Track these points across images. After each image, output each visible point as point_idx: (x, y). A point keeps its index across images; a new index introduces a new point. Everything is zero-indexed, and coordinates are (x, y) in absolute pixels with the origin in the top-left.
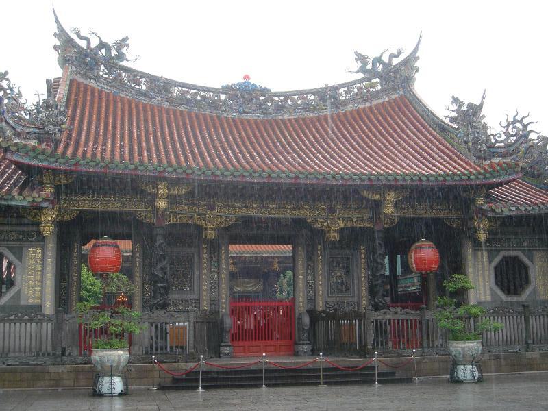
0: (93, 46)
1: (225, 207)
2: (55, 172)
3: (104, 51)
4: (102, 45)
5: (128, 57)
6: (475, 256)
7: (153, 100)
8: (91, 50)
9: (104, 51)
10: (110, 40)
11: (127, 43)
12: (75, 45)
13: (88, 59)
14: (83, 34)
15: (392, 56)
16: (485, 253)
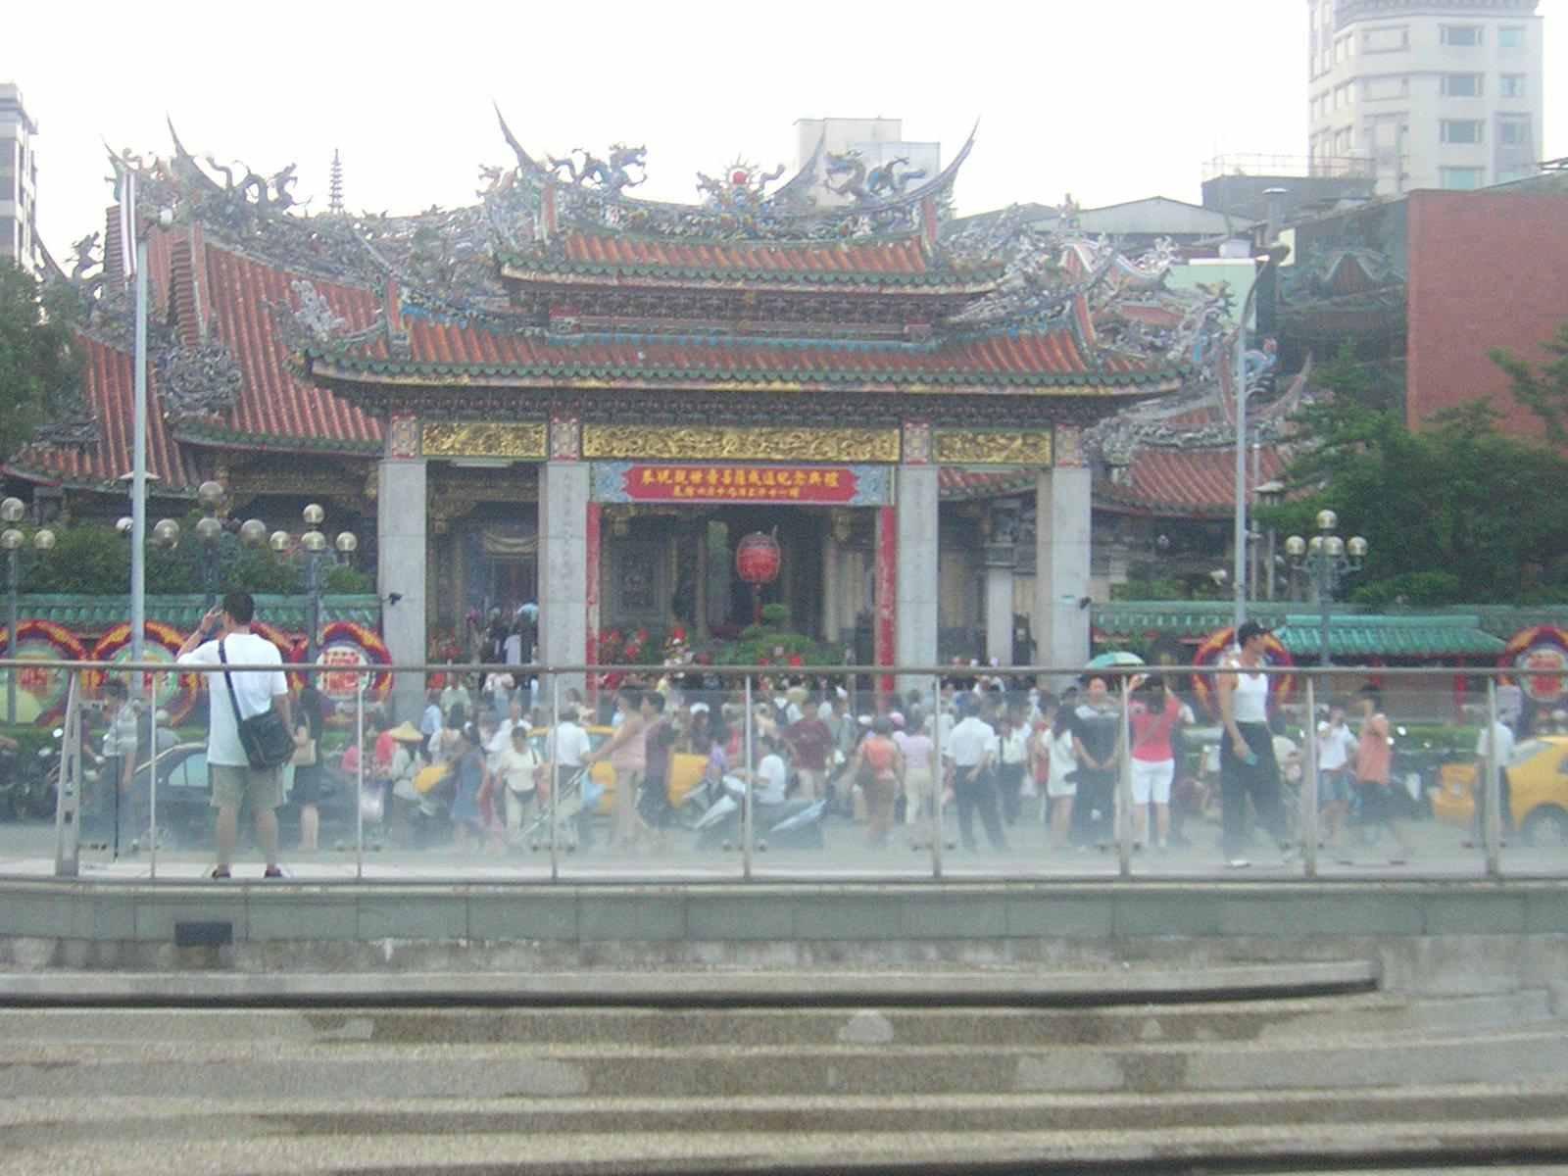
0: (236, 182)
1: (460, 487)
2: (230, 452)
3: (254, 189)
4: (252, 179)
5: (295, 200)
6: (839, 559)
7: (341, 278)
8: (235, 191)
9: (254, 189)
10: (267, 172)
11: (292, 175)
12: (211, 185)
13: (230, 209)
14: (219, 163)
15: (766, 178)
16: (860, 555)
